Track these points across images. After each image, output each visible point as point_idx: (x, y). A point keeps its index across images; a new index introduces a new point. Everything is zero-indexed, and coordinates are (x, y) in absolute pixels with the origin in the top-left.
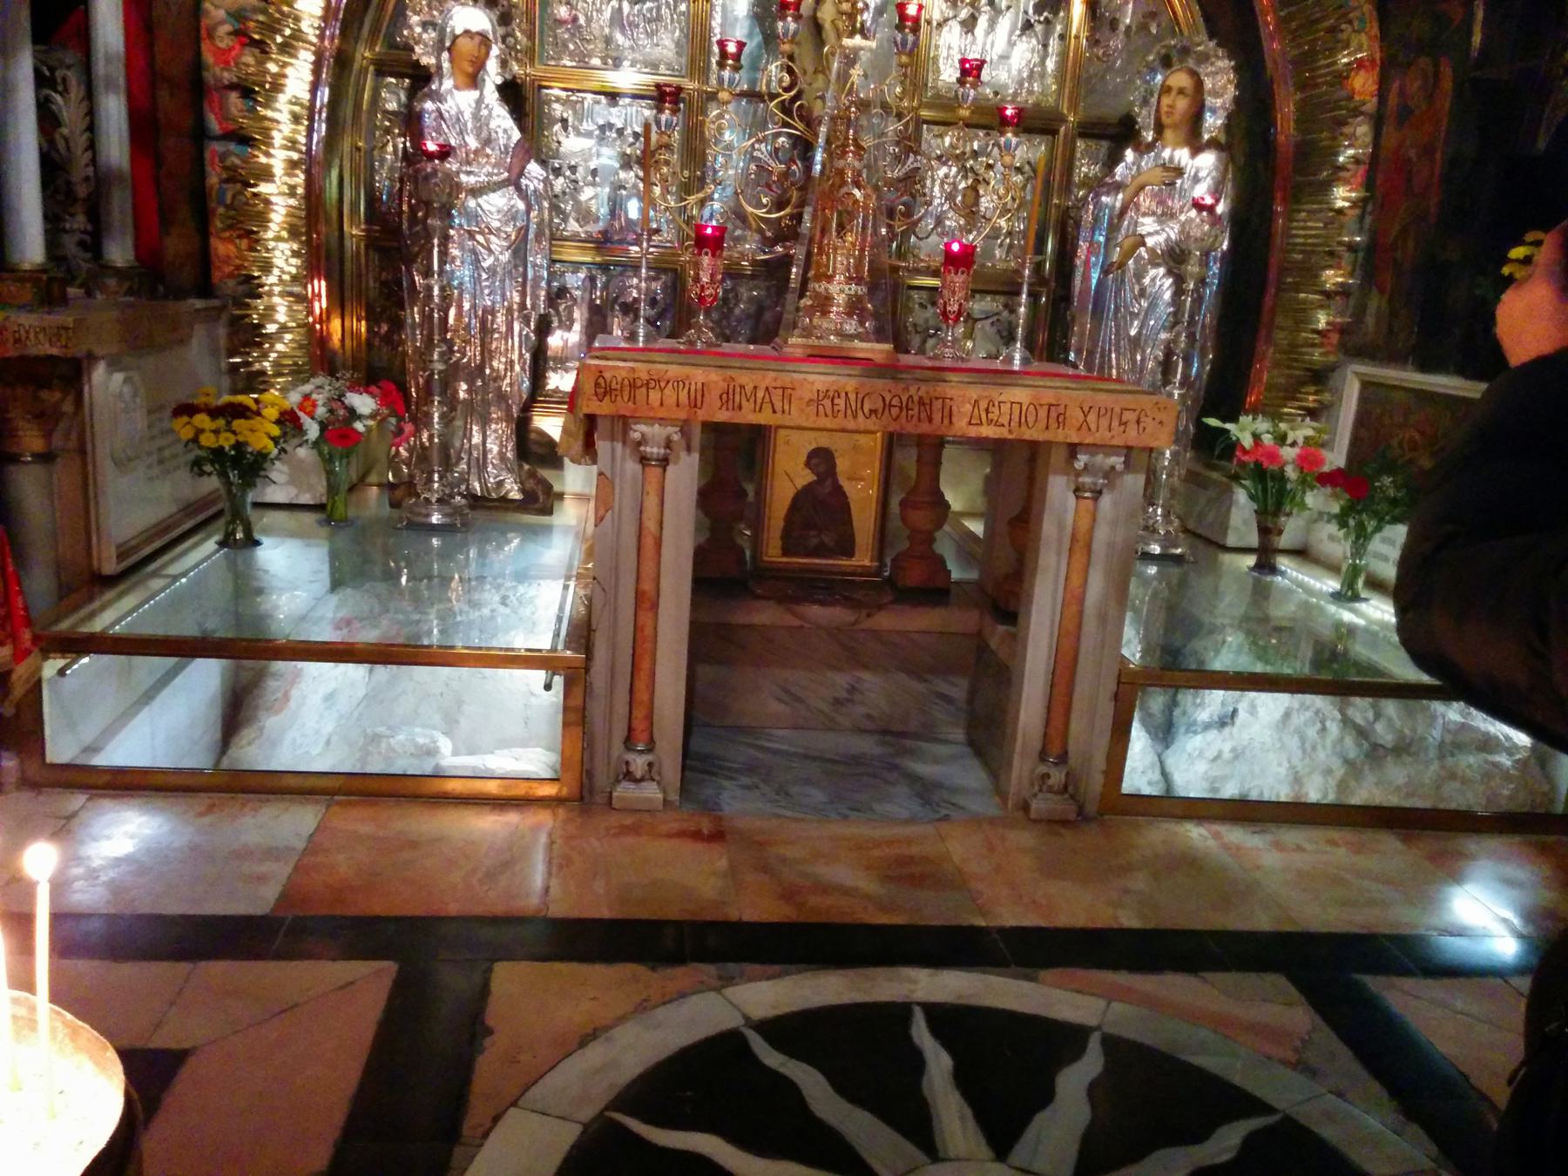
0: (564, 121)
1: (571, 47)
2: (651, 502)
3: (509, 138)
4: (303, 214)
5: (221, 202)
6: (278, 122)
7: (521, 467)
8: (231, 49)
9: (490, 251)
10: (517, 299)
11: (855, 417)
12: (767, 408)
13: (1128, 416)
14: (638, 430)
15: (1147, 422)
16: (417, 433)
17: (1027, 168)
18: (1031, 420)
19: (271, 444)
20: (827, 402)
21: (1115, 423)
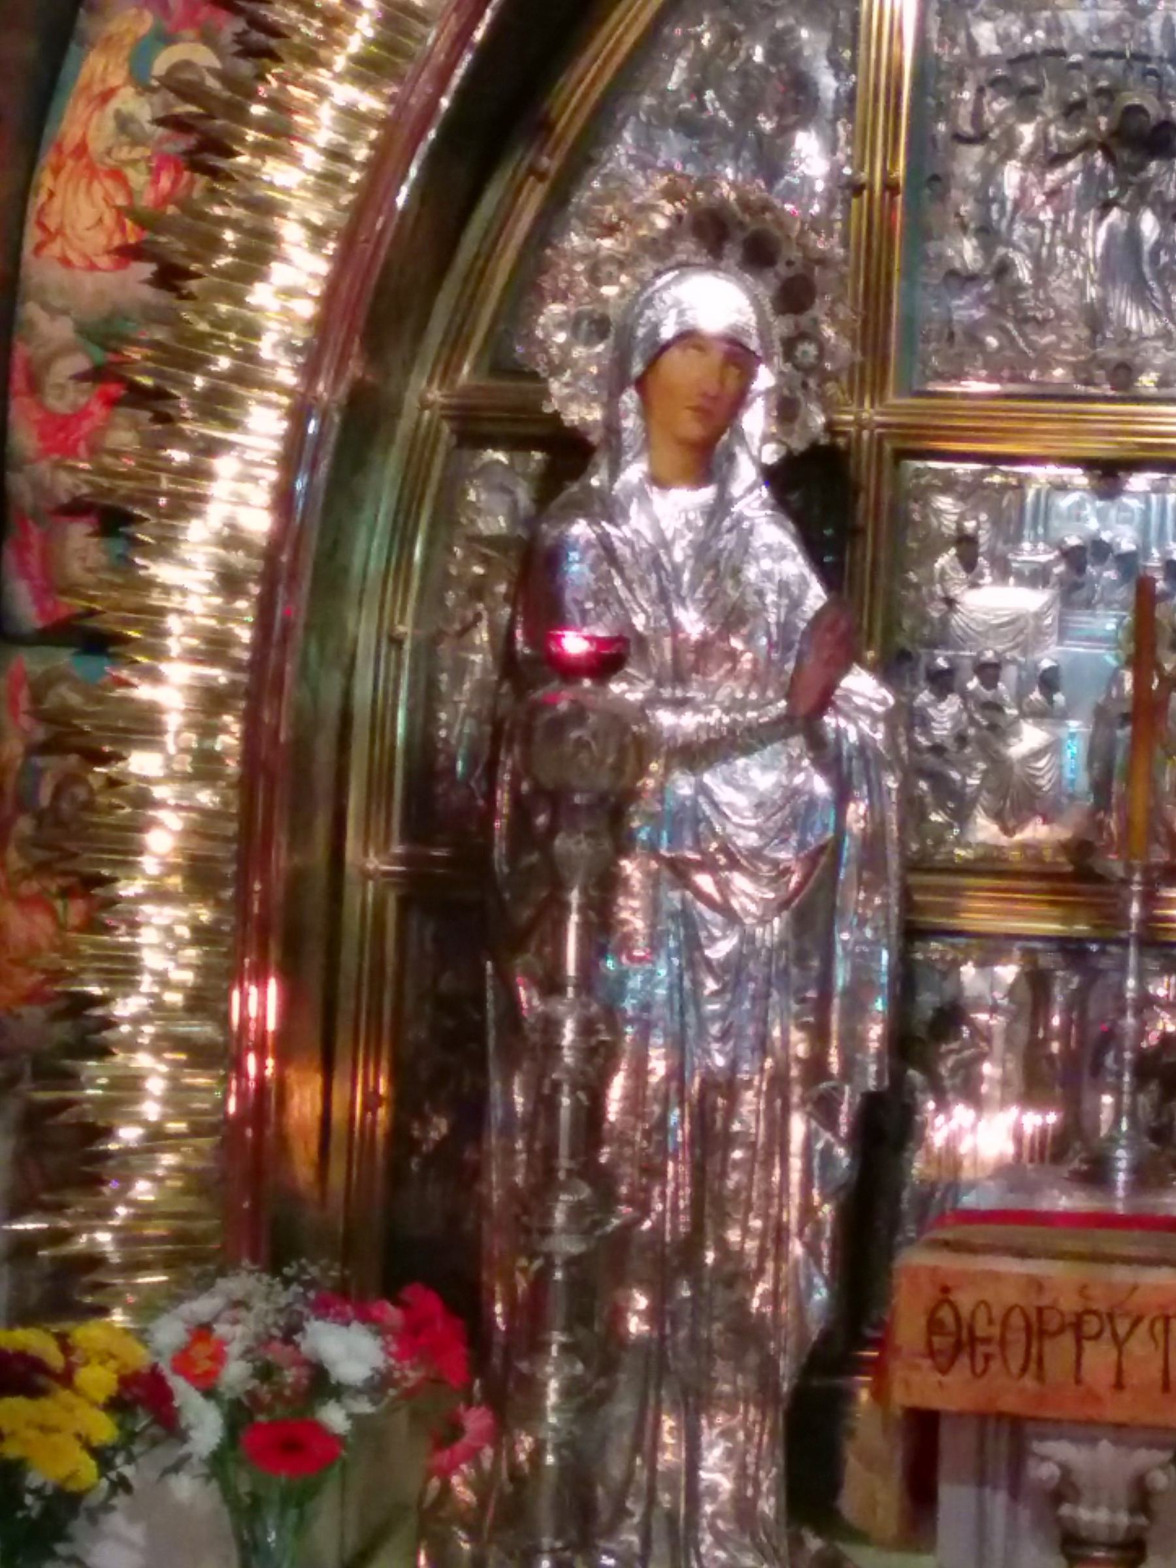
0: (966, 544)
1: (992, 341)
3: (796, 604)
4: (232, 828)
5: (24, 804)
6: (184, 591)
7: (797, 1542)
8: (83, 414)
9: (731, 917)
10: (800, 1047)
16: (500, 1433)
19: (88, 1468)
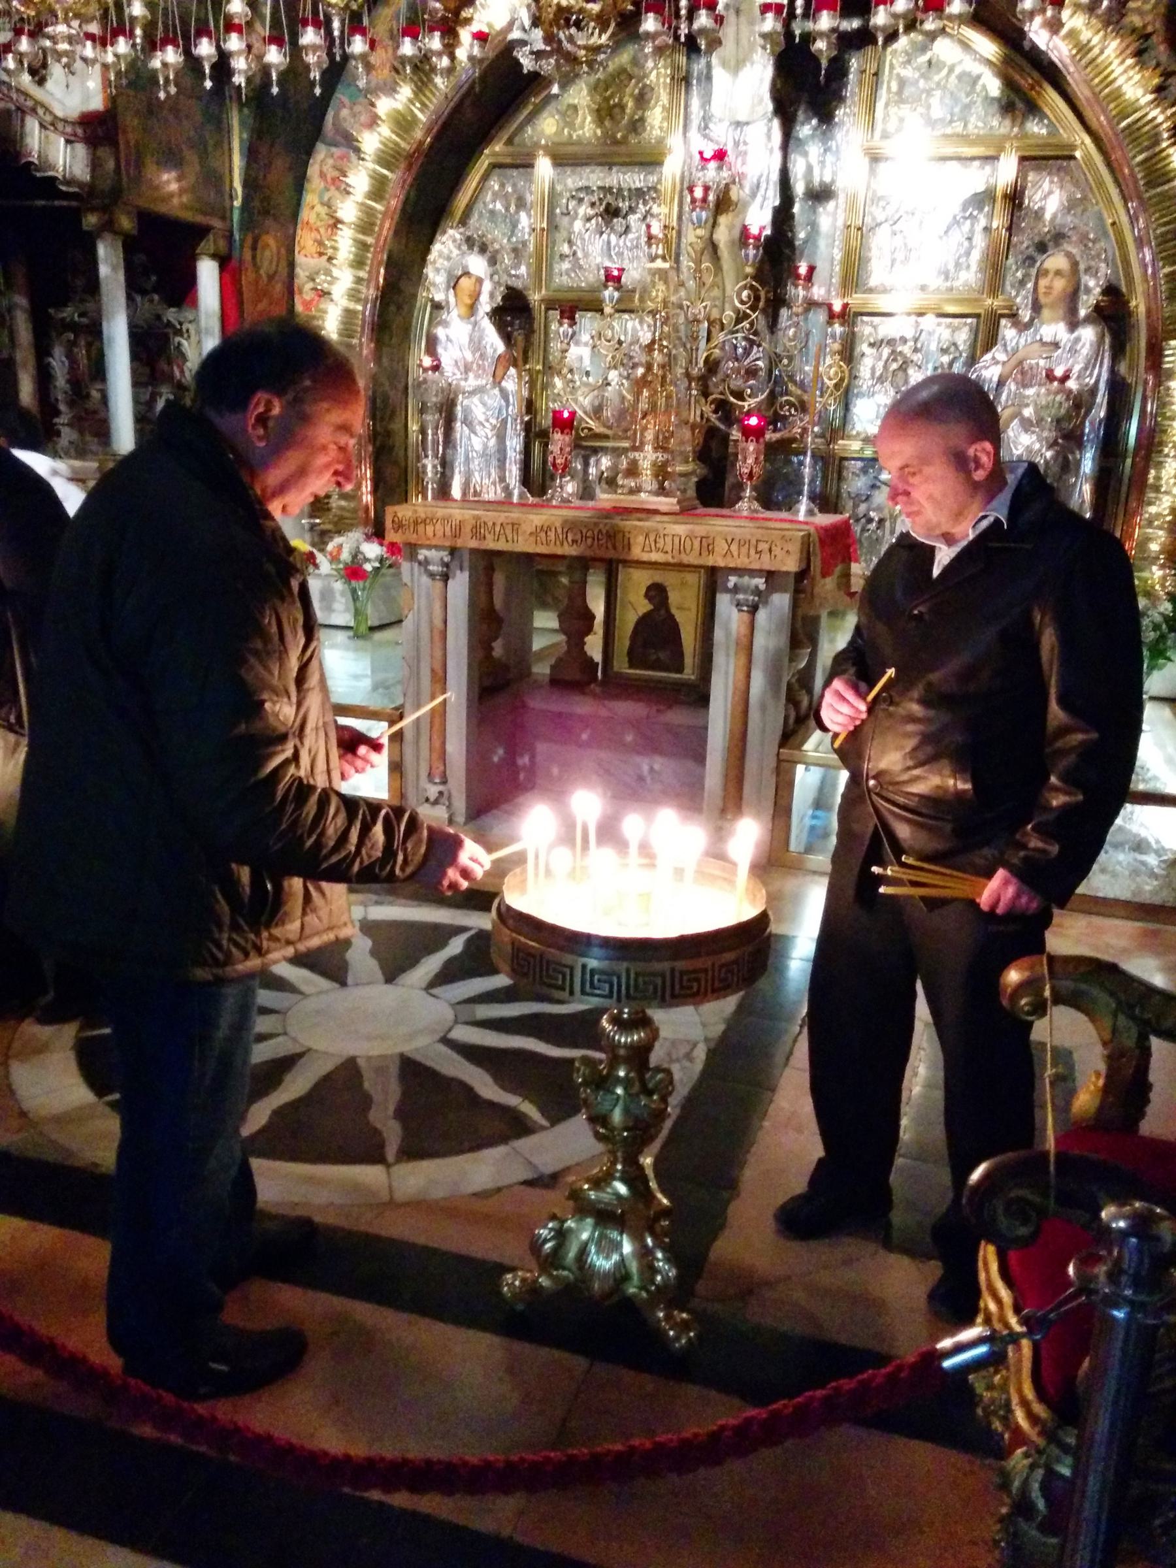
2: (437, 606)
8: (312, 300)
11: (562, 544)
12: (503, 539)
13: (763, 546)
14: (423, 554)
15: (777, 551)
17: (952, 349)
18: (688, 548)
20: (543, 535)
21: (752, 552)
